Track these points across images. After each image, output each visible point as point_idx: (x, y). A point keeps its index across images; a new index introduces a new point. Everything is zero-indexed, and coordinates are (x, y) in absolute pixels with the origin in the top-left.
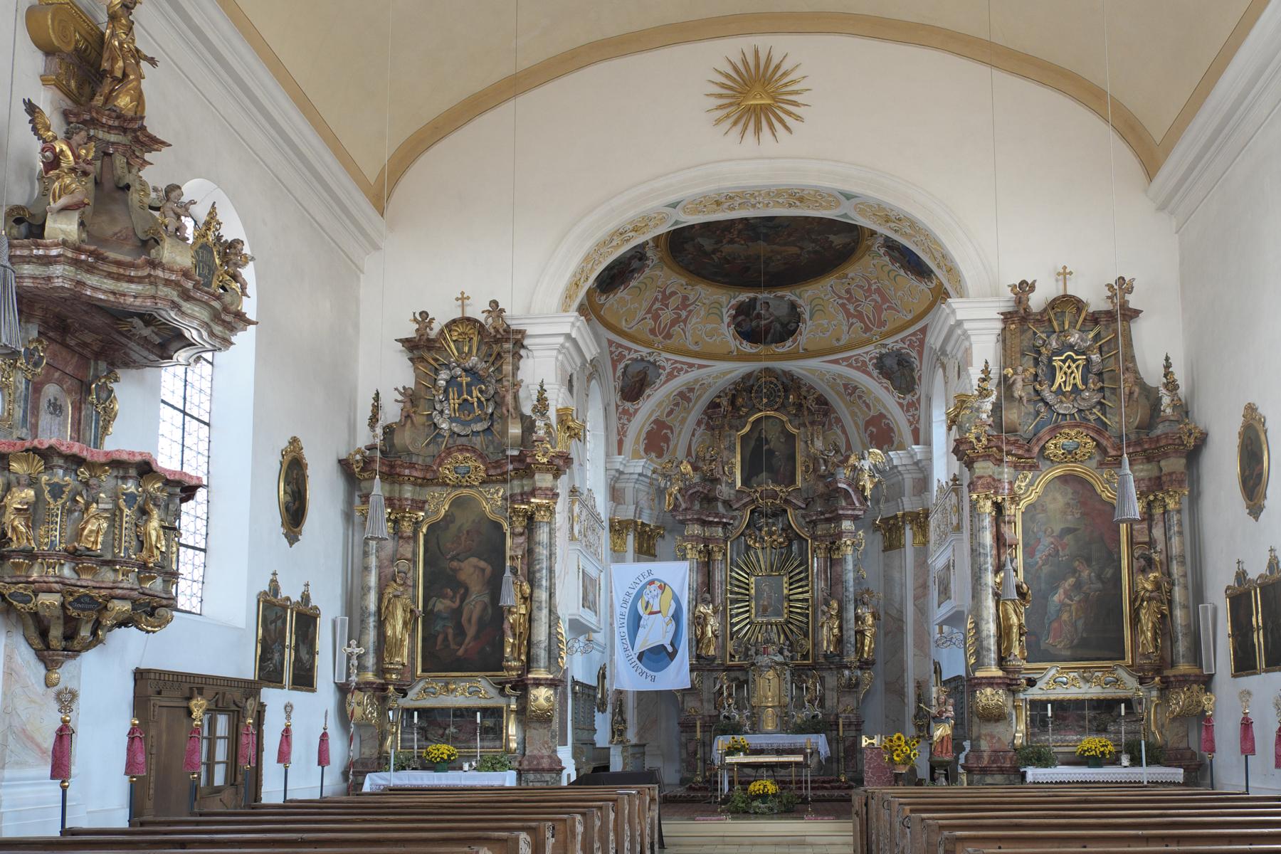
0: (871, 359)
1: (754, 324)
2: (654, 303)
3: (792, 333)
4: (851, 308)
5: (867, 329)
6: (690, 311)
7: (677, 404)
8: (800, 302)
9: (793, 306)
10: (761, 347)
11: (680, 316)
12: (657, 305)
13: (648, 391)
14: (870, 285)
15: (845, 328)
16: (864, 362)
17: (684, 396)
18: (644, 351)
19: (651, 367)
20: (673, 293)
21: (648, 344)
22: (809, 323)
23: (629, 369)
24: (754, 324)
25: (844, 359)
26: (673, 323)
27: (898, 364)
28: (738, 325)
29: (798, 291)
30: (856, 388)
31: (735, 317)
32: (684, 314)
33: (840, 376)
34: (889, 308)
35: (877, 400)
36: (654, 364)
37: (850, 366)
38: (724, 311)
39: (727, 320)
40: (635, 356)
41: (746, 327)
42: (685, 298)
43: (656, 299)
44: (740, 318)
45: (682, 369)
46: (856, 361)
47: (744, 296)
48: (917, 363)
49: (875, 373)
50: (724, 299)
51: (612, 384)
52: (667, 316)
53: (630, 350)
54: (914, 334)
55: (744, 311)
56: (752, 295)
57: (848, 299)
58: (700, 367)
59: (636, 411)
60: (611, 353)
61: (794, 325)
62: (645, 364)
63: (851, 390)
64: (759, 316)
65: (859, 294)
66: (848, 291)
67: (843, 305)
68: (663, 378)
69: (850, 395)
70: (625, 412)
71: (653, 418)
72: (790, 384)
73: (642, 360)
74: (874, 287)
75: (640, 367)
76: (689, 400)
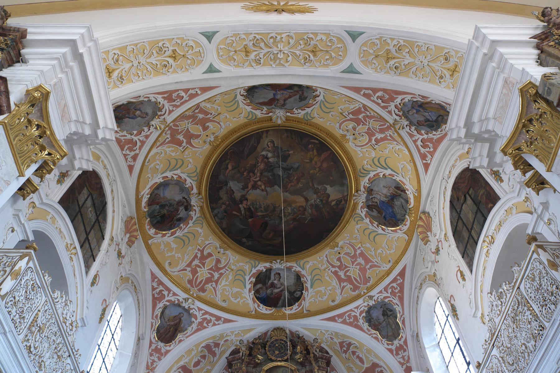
0: (361, 313)
1: (269, 291)
2: (193, 260)
3: (298, 299)
4: (342, 274)
5: (355, 288)
6: (221, 274)
7: (204, 357)
8: (303, 272)
9: (298, 277)
10: (274, 309)
11: (213, 276)
12: (196, 262)
13: (180, 336)
14: (355, 251)
15: (338, 291)
16: (355, 317)
17: (210, 349)
18: (182, 295)
19: (185, 314)
20: (210, 255)
21: (186, 291)
22: (310, 290)
23: (167, 312)
24: (269, 291)
25: (340, 316)
26: (208, 281)
27: (384, 315)
28: (257, 292)
29: (302, 262)
30: (350, 344)
31: (255, 285)
32: (216, 275)
33: (337, 334)
34: (371, 267)
35: (369, 351)
36: (187, 311)
37: (344, 322)
38: (247, 278)
39: (248, 286)
40: (173, 299)
41: (263, 294)
42: (218, 261)
43: (196, 256)
44: (259, 286)
45: (210, 321)
46: (349, 316)
47: (262, 267)
48: (398, 309)
49: (366, 326)
50: (247, 267)
51: (150, 320)
52: (203, 273)
53: (169, 290)
54: (395, 280)
55: (262, 279)
56: (268, 265)
57: (339, 267)
58: (227, 321)
59: (167, 352)
60: (153, 289)
61: (299, 293)
62: (180, 310)
63: (346, 346)
64: (273, 285)
65: (347, 261)
66: (339, 259)
67: (335, 273)
68: (194, 326)
69: (345, 352)
70: (157, 350)
71: (182, 363)
72: (297, 340)
73: (179, 305)
74: (359, 252)
75: (178, 311)
76: (214, 354)
